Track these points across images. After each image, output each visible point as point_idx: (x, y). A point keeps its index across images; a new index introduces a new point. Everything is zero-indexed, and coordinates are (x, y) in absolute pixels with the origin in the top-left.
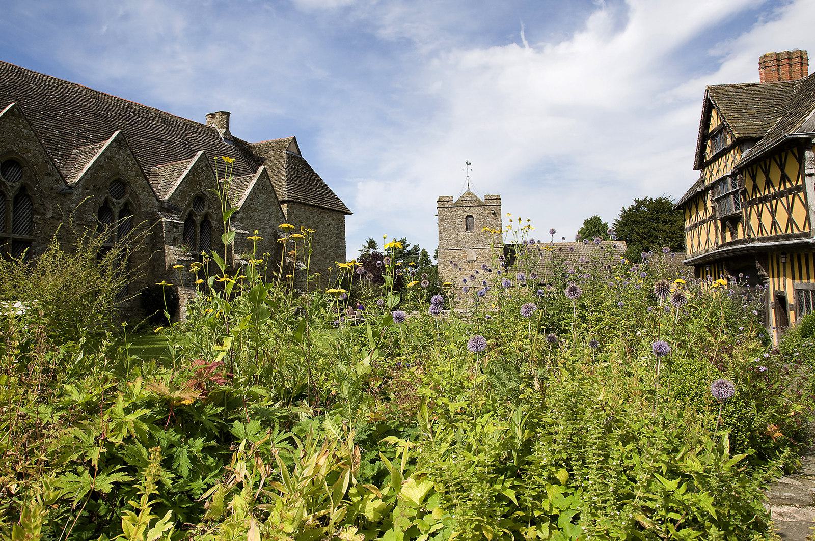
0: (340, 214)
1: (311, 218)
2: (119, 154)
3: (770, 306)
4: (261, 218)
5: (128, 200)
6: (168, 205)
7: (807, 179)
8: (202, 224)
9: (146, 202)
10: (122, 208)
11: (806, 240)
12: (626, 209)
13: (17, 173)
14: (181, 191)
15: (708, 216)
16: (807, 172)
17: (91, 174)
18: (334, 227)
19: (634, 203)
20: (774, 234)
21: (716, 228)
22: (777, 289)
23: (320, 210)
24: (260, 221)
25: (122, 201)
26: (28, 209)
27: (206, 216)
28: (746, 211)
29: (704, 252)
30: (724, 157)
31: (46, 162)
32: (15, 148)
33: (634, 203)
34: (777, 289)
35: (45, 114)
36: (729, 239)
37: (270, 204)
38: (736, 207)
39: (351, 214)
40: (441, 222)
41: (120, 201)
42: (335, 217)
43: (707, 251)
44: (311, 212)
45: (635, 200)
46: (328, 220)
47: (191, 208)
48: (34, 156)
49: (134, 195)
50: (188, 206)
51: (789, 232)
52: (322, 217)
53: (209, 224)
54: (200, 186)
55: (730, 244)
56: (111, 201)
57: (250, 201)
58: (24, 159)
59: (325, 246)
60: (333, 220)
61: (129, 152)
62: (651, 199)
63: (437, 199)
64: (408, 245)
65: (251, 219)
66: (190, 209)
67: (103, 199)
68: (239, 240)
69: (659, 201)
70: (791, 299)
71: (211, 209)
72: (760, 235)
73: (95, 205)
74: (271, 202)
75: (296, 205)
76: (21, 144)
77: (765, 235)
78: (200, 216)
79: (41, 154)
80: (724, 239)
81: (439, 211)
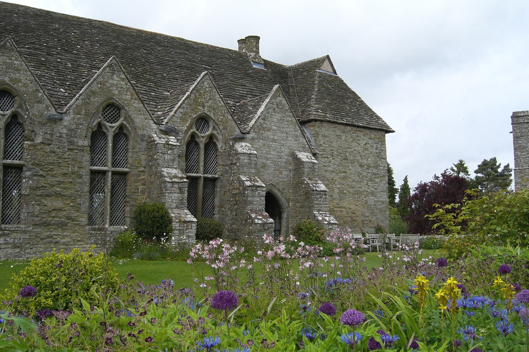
0: (380, 133)
1: (343, 137)
2: (113, 79)
4: (276, 138)
5: (123, 124)
6: (165, 127)
8: (207, 146)
9: (143, 125)
10: (117, 131)
13: (10, 102)
14: (181, 113)
17: (83, 99)
18: (372, 146)
23: (354, 128)
24: (274, 141)
25: (116, 124)
26: (20, 135)
27: (211, 137)
31: (37, 90)
32: (7, 79)
35: (62, 49)
37: (286, 123)
39: (394, 132)
40: (516, 139)
41: (113, 125)
42: (373, 136)
44: (344, 132)
46: (364, 138)
47: (194, 130)
48: (25, 85)
49: (128, 118)
50: (190, 127)
52: (357, 136)
53: (215, 145)
54: (204, 107)
56: (105, 126)
57: (262, 121)
58: (15, 89)
59: (362, 166)
60: (371, 139)
61: (123, 76)
63: (511, 114)
64: (499, 167)
65: (263, 140)
66: (192, 131)
67: (95, 123)
68: (245, 161)
71: (216, 130)
73: (87, 130)
74: (287, 121)
75: (325, 124)
76: (12, 74)
78: (203, 137)
79: (31, 83)
81: (513, 127)
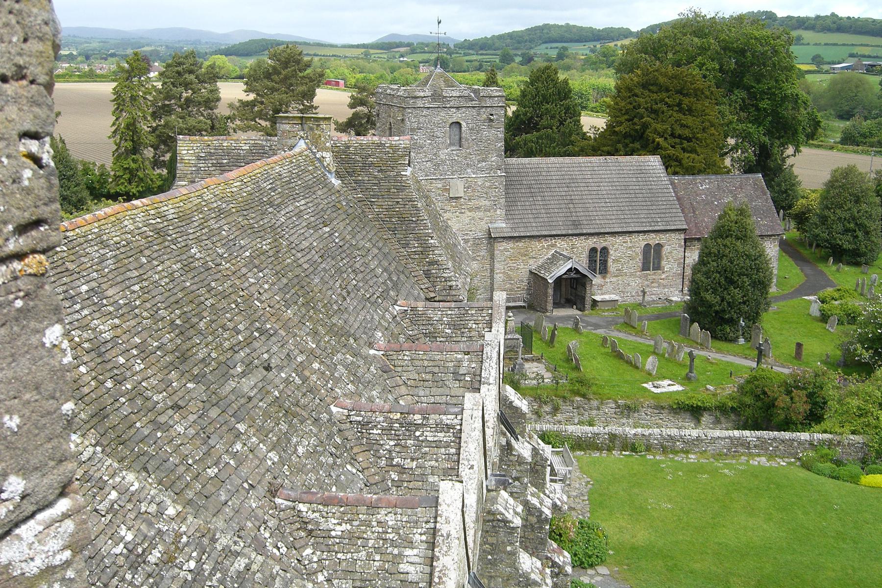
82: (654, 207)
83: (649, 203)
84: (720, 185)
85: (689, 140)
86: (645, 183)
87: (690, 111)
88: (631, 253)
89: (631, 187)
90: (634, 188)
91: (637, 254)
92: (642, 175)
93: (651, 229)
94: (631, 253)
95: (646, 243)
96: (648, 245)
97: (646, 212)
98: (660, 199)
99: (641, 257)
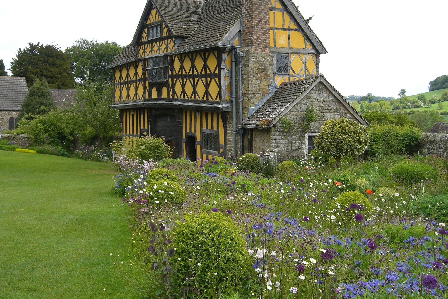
3: (183, 141)
7: (222, 71)
11: (218, 106)
12: (22, 50)
15: (138, 78)
16: (222, 67)
19: (28, 46)
20: (193, 98)
21: (145, 87)
22: (188, 131)
28: (172, 81)
29: (132, 102)
30: (158, 43)
33: (28, 46)
34: (188, 131)
36: (155, 95)
38: (164, 77)
43: (135, 102)
45: (30, 44)
51: (205, 99)
55: (155, 100)
62: (42, 45)
69: (49, 47)
70: (199, 138)
72: (182, 97)
77: (186, 98)
80: (150, 95)
82: (17, 100)
83: (14, 98)
84: (60, 94)
85: (52, 78)
86: (13, 89)
87: (54, 65)
88: (2, 122)
89: (5, 90)
90: (7, 90)
91: (5, 123)
92: (13, 85)
93: (13, 109)
94: (2, 122)
95: (11, 117)
96: (12, 118)
97: (12, 101)
98: (21, 96)
99: (8, 124)
